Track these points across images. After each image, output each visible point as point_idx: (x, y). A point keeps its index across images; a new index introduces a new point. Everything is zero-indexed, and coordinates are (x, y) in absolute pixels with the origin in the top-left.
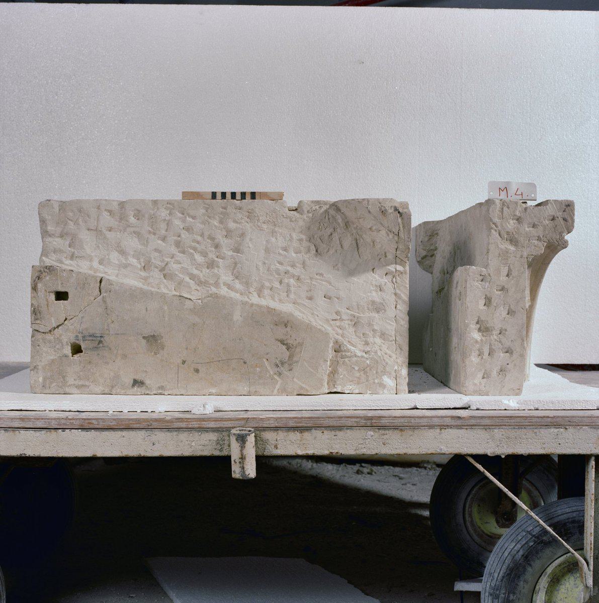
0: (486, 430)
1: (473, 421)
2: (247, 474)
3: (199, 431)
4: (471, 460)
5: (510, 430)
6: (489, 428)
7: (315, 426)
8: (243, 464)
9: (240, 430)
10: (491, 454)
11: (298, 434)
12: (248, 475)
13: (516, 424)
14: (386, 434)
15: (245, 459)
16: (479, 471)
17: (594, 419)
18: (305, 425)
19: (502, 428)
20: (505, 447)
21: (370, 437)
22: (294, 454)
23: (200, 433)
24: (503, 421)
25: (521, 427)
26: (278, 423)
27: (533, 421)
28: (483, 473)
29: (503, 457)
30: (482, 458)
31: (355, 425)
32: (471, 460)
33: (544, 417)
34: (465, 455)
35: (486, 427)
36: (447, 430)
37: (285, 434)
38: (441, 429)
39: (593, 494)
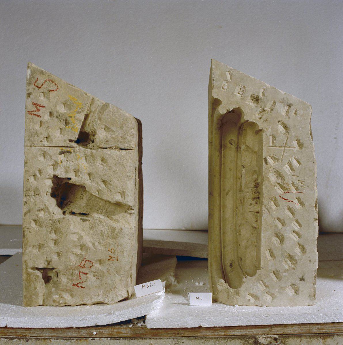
3: (225, 338)
7: (337, 332)
9: (265, 338)
11: (321, 340)
18: (328, 331)
23: (226, 341)
37: (309, 340)
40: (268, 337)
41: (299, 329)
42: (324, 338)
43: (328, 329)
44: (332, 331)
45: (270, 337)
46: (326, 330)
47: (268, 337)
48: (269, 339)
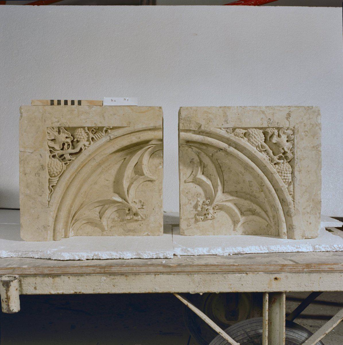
0: (188, 275)
1: (179, 269)
2: (11, 309)
4: (179, 297)
5: (206, 275)
6: (191, 274)
7: (63, 273)
8: (8, 302)
9: (8, 277)
10: (192, 292)
12: (13, 310)
13: (210, 270)
14: (115, 279)
15: (9, 299)
16: (184, 304)
17: (268, 266)
18: (56, 272)
19: (200, 274)
20: (203, 287)
21: (103, 281)
22: (49, 294)
24: (201, 268)
25: (214, 273)
26: (36, 271)
27: (223, 268)
28: (186, 307)
29: (201, 294)
30: (187, 296)
31: (93, 272)
32: (179, 297)
33: (231, 265)
34: (173, 293)
35: (189, 273)
36: (160, 275)
37: (42, 279)
38: (155, 275)
39: (267, 321)
40: (10, 277)
41: (35, 270)
42: (53, 278)
43: (56, 271)
44: (60, 272)
45: (12, 277)
46: (55, 272)
47: (10, 277)
48: (11, 278)
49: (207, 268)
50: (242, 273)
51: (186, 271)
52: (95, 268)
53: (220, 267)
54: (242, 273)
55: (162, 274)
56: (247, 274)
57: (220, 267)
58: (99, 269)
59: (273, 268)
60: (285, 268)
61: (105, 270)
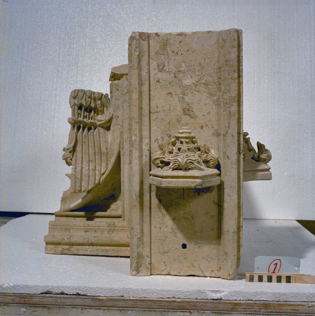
0: (121, 311)
13: (147, 306)
17: (217, 304)
19: (135, 310)
24: (136, 304)
36: (88, 310)
49: (143, 303)
50: (185, 312)
51: (118, 305)
52: (14, 297)
53: (158, 303)
54: (185, 312)
55: (91, 308)
56: (190, 312)
57: (159, 302)
58: (19, 298)
59: (222, 306)
60: (237, 307)
61: (26, 299)
